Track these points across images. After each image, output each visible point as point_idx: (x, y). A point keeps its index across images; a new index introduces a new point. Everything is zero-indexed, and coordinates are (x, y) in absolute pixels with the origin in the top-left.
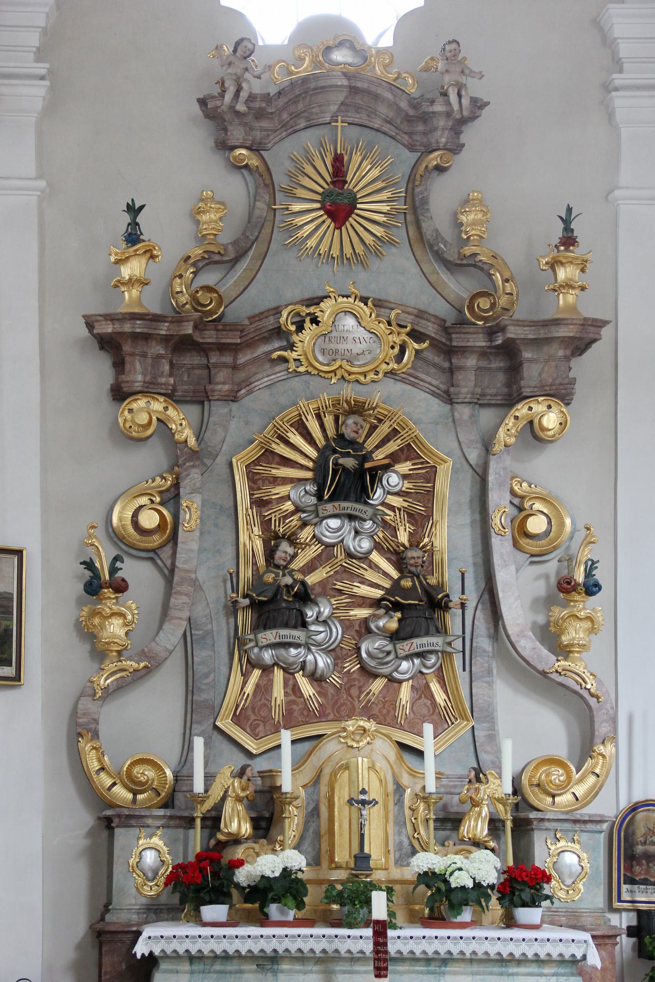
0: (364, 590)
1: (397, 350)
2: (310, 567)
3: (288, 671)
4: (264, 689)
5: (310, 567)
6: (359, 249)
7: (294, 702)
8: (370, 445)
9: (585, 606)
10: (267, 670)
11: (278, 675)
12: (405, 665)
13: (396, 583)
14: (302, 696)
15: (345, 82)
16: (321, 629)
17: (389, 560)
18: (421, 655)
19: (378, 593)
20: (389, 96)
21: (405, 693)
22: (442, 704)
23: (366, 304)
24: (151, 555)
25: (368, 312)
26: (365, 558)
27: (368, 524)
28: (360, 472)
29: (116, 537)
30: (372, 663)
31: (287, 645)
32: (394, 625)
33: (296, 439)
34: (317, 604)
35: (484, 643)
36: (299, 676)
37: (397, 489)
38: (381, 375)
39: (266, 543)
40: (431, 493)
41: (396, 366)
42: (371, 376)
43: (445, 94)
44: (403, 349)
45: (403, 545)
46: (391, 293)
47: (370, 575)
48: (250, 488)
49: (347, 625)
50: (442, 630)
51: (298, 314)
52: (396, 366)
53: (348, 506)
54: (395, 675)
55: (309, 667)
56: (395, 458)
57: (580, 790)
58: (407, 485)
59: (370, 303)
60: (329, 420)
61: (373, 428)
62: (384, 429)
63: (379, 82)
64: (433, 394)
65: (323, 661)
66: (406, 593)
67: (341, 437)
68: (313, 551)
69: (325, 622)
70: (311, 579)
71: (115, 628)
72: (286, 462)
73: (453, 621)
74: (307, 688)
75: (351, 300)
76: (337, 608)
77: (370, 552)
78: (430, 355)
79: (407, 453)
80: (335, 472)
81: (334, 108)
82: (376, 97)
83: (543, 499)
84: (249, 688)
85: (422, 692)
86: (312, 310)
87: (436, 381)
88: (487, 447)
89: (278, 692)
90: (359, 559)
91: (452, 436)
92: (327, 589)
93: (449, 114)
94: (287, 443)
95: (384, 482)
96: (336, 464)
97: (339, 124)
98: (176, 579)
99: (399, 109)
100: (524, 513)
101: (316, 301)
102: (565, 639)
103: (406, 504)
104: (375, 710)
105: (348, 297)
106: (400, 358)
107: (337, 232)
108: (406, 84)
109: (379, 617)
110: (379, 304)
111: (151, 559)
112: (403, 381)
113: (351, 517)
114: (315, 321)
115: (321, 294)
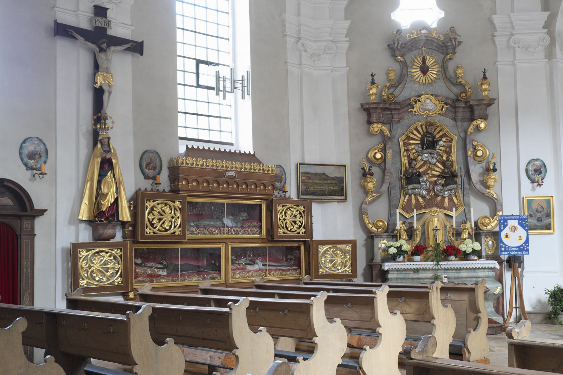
0: (435, 173)
1: (441, 108)
2: (421, 167)
3: (416, 196)
4: (409, 200)
5: (421, 167)
6: (430, 81)
7: (417, 204)
8: (435, 133)
10: (410, 195)
11: (413, 197)
12: (446, 193)
13: (443, 171)
14: (419, 202)
15: (425, 38)
16: (424, 184)
17: (441, 164)
18: (451, 190)
19: (438, 173)
20: (436, 41)
21: (446, 200)
22: (456, 203)
24: (379, 165)
25: (433, 98)
26: (435, 164)
27: (435, 155)
28: (433, 141)
29: (369, 160)
30: (438, 193)
31: (415, 189)
32: (443, 182)
33: (415, 132)
34: (423, 177)
35: (467, 186)
36: (418, 197)
37: (443, 145)
38: (437, 115)
39: (409, 161)
40: (451, 146)
41: (441, 112)
42: (435, 115)
43: (451, 41)
44: (443, 107)
45: (445, 160)
46: (439, 92)
48: (404, 146)
49: (431, 182)
50: (455, 183)
51: (415, 99)
52: (441, 112)
53: (430, 151)
54: (444, 195)
55: (421, 194)
56: (442, 137)
58: (445, 144)
60: (424, 127)
61: (436, 129)
62: (438, 129)
63: (434, 38)
64: (451, 119)
65: (425, 192)
66: (446, 173)
67: (427, 132)
68: (421, 163)
69: (425, 182)
70: (421, 170)
71: (370, 185)
72: (413, 139)
73: (458, 180)
74: (421, 200)
75: (429, 95)
77: (436, 163)
78: (450, 109)
79: (445, 135)
80: (426, 142)
82: (433, 41)
84: (406, 201)
85: (451, 199)
86: (419, 98)
87: (451, 115)
89: (413, 201)
90: (433, 165)
91: (456, 130)
92: (425, 173)
93: (452, 45)
94: (413, 134)
95: (439, 143)
96: (427, 139)
97: (424, 49)
98: (386, 172)
99: (439, 44)
101: (420, 96)
103: (445, 149)
104: (439, 205)
105: (428, 94)
106: (442, 110)
107: (424, 77)
108: (441, 38)
109: (439, 180)
110: (436, 96)
111: (379, 166)
112: (443, 115)
113: (431, 154)
114: (419, 101)
115: (421, 94)
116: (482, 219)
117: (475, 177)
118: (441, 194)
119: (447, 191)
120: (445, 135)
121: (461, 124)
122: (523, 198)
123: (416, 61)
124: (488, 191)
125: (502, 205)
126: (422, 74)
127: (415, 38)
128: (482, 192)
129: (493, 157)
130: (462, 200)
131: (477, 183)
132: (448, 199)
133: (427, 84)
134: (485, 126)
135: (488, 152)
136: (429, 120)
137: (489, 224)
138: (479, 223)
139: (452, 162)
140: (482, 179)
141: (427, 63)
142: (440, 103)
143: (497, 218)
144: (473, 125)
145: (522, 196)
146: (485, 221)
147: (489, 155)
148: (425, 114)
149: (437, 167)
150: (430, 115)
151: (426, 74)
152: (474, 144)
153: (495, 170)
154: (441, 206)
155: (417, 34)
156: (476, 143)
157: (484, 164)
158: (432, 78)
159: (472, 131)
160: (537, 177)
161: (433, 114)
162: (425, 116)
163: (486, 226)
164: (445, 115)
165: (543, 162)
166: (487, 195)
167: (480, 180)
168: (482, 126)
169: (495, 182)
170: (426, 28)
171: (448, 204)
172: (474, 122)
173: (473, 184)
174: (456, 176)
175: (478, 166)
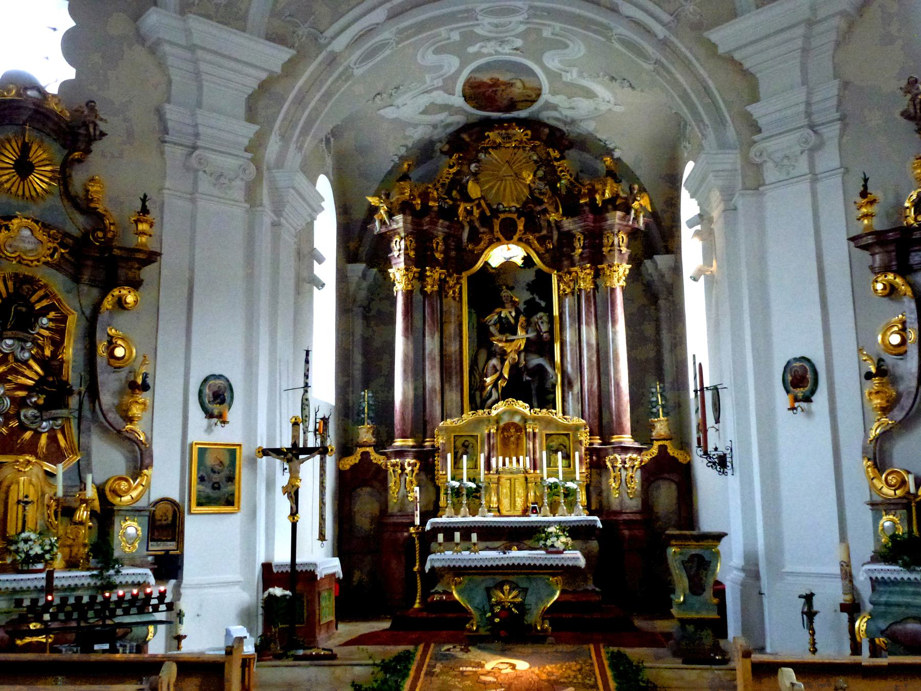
0: (23, 380)
1: (51, 251)
9: (143, 397)
12: (44, 424)
15: (34, 107)
22: (42, 445)
23: (37, 224)
25: (38, 229)
27: (29, 344)
35: (87, 413)
37: (45, 326)
38: (41, 263)
41: (49, 259)
44: (55, 250)
45: (48, 357)
47: (27, 372)
49: (13, 400)
50: (66, 406)
52: (49, 259)
54: (39, 430)
57: (134, 494)
58: (51, 324)
59: (40, 224)
62: (41, 293)
73: (73, 401)
75: (29, 221)
76: (8, 390)
79: (52, 308)
81: (25, 118)
83: (122, 339)
88: (96, 308)
91: (76, 301)
95: (39, 322)
97: (27, 127)
100: (112, 346)
102: (130, 414)
103: (50, 335)
107: (22, 183)
116: (115, 480)
117: (107, 399)
118: (33, 426)
119: (45, 420)
120: (52, 308)
121: (88, 290)
122: (191, 445)
123: (8, 147)
124: (129, 426)
125: (151, 457)
126: (17, 176)
127: (12, 101)
128: (118, 428)
129: (143, 363)
130: (76, 441)
131: (110, 410)
132: (48, 437)
133: (27, 198)
134: (136, 302)
135: (134, 351)
136: (24, 271)
137: (127, 492)
138: (107, 489)
139: (62, 362)
140: (116, 402)
141: (30, 156)
142: (50, 241)
143: (142, 481)
144: (113, 296)
145: (189, 441)
146: (119, 485)
147: (136, 357)
148: (15, 258)
149: (30, 367)
150: (25, 262)
151: (26, 179)
152: (109, 332)
153: (145, 387)
154: (31, 448)
155: (18, 94)
156: (113, 330)
157: (123, 374)
158: (39, 189)
159: (110, 307)
160: (216, 409)
161: (32, 261)
162: (14, 262)
163: (121, 497)
164: (57, 267)
165: (228, 381)
166: (128, 435)
167: (114, 404)
168: (130, 299)
169: (144, 410)
170: (40, 90)
171: (46, 448)
172: (115, 290)
173: (101, 409)
174: (70, 392)
175: (113, 376)
